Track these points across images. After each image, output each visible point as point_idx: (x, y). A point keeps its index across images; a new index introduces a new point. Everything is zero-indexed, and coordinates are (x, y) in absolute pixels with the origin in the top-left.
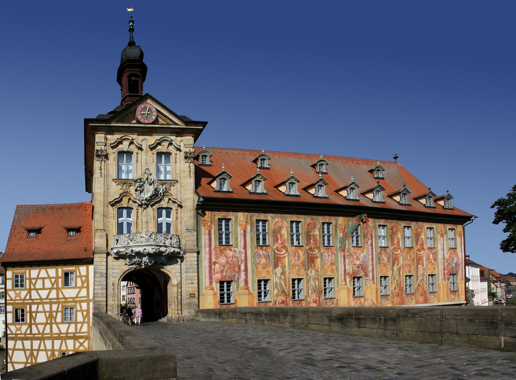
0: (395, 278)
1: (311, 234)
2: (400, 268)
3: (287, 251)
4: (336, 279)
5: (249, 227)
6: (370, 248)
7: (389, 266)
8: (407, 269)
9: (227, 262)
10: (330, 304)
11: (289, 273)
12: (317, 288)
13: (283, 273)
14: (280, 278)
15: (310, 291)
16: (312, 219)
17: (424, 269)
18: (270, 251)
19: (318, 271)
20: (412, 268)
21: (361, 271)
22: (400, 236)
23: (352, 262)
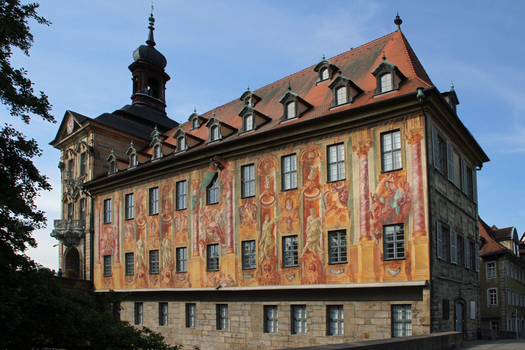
0: (264, 242)
1: (166, 198)
2: (273, 225)
3: (146, 222)
4: (188, 248)
5: (121, 203)
6: (229, 201)
7: (255, 225)
8: (285, 225)
9: (108, 239)
10: (182, 279)
11: (147, 245)
12: (170, 260)
13: (143, 245)
14: (140, 251)
15: (164, 264)
16: (167, 181)
17: (319, 222)
18: (134, 223)
19: (170, 241)
20: (295, 224)
21: (217, 235)
23: (206, 225)
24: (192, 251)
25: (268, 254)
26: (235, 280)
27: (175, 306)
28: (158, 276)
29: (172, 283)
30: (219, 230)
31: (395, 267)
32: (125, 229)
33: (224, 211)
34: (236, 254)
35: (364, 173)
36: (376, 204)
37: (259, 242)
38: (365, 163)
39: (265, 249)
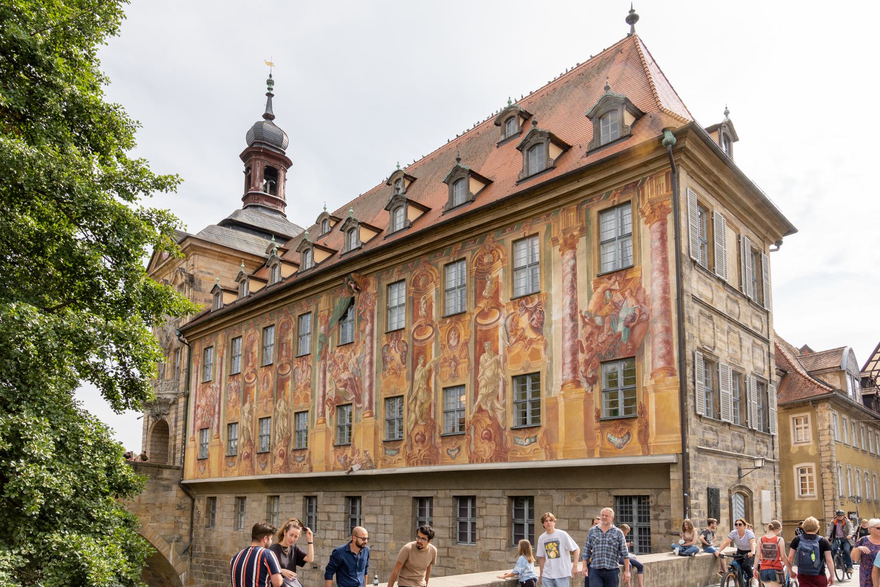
0: (416, 398)
2: (430, 371)
6: (368, 339)
7: (404, 373)
8: (447, 370)
15: (277, 437)
19: (287, 402)
20: (463, 366)
21: (350, 391)
22: (433, 293)
23: (335, 377)
24: (316, 417)
25: (421, 416)
26: (373, 459)
27: (289, 500)
28: (269, 456)
29: (286, 467)
30: (353, 384)
31: (620, 432)
32: (229, 388)
33: (361, 353)
34: (376, 419)
35: (570, 280)
36: (589, 329)
37: (408, 399)
38: (572, 263)
39: (417, 408)
